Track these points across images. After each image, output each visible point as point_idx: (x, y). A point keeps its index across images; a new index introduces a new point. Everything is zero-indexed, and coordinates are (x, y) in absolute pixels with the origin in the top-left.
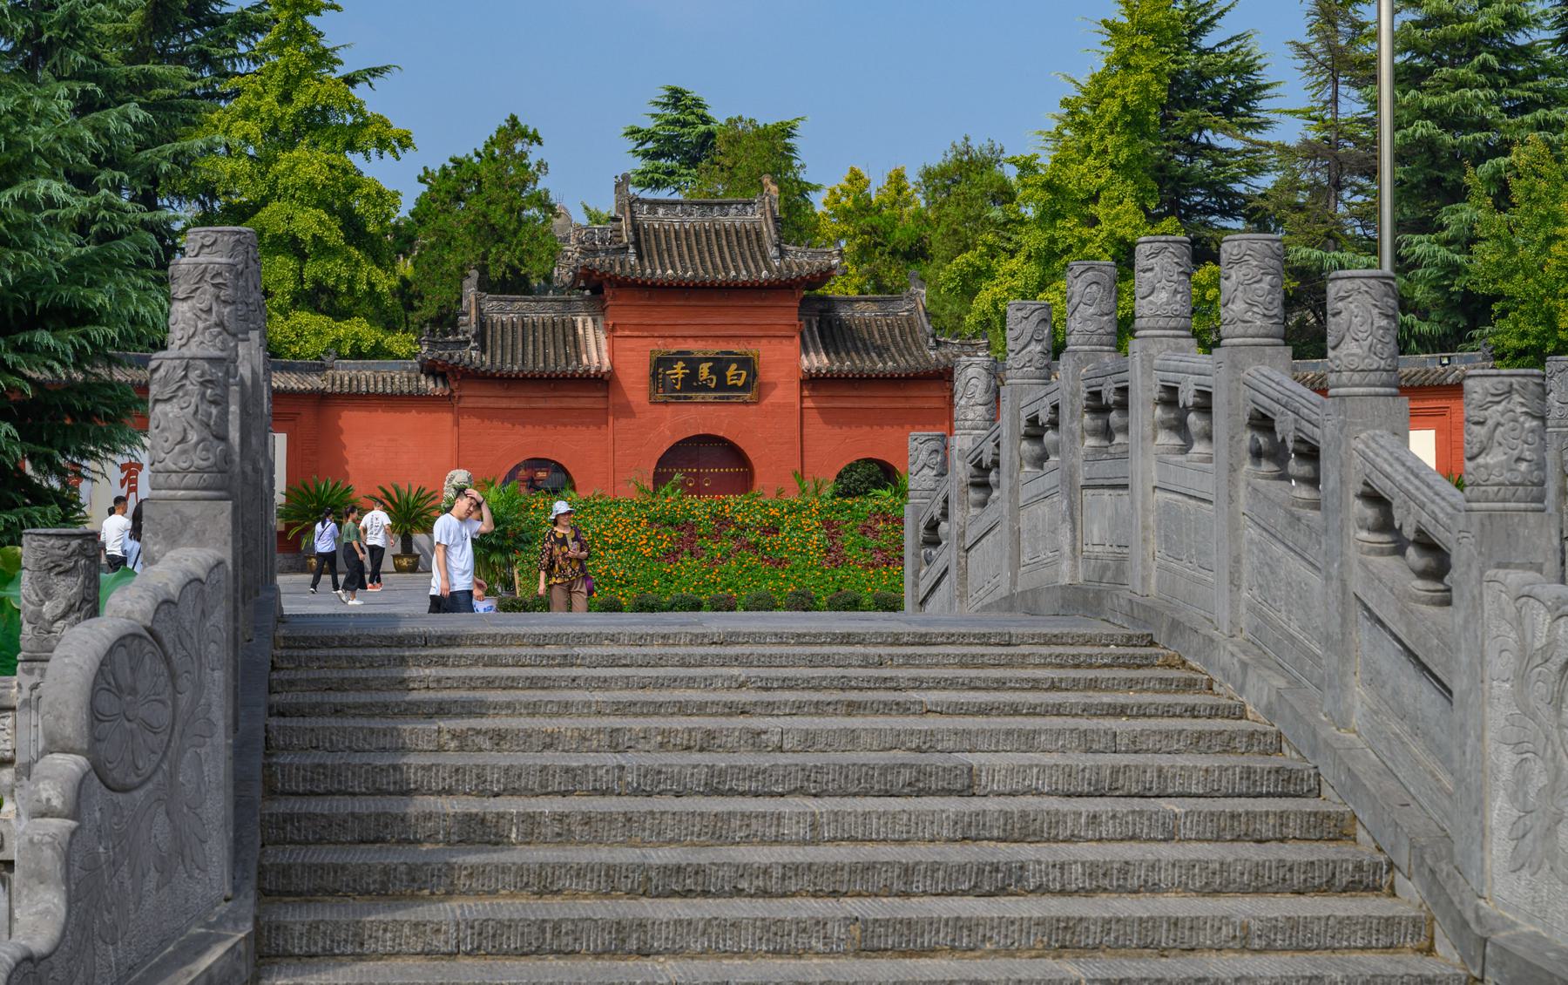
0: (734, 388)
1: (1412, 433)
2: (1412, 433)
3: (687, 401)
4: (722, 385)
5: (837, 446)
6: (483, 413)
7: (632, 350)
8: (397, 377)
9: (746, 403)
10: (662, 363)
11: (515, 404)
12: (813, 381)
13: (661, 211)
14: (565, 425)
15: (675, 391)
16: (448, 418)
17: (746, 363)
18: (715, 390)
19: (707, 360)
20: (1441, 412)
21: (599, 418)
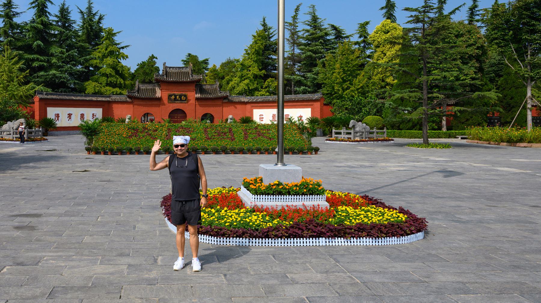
1: (254, 110)
2: (254, 110)
5: (201, 111)
8: (123, 98)
10: (170, 96)
12: (197, 99)
16: (132, 106)
17: (185, 96)
20: (312, 105)
21: (159, 106)
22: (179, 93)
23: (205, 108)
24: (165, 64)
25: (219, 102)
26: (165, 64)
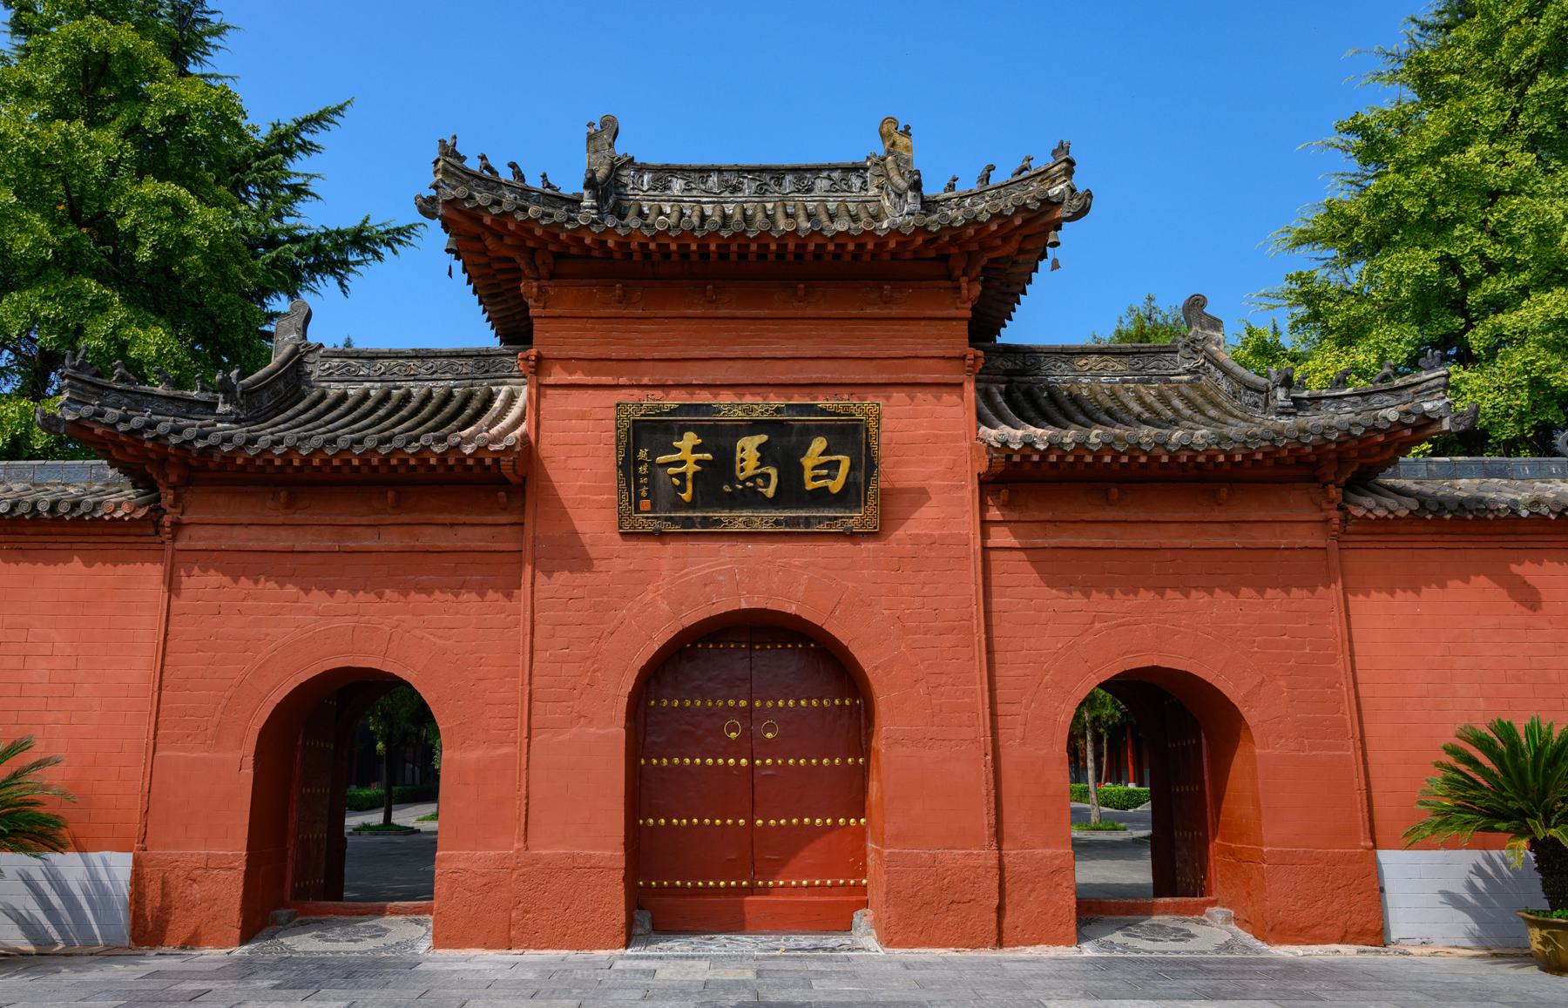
0: (821, 497)
3: (711, 532)
4: (792, 492)
6: (237, 563)
7: (582, 416)
9: (851, 536)
10: (644, 436)
11: (304, 541)
13: (677, 185)
14: (428, 591)
15: (679, 505)
16: (148, 576)
18: (774, 503)
19: (754, 427)
21: (501, 573)
22: (764, 404)
23: (1123, 604)
25: (1295, 525)
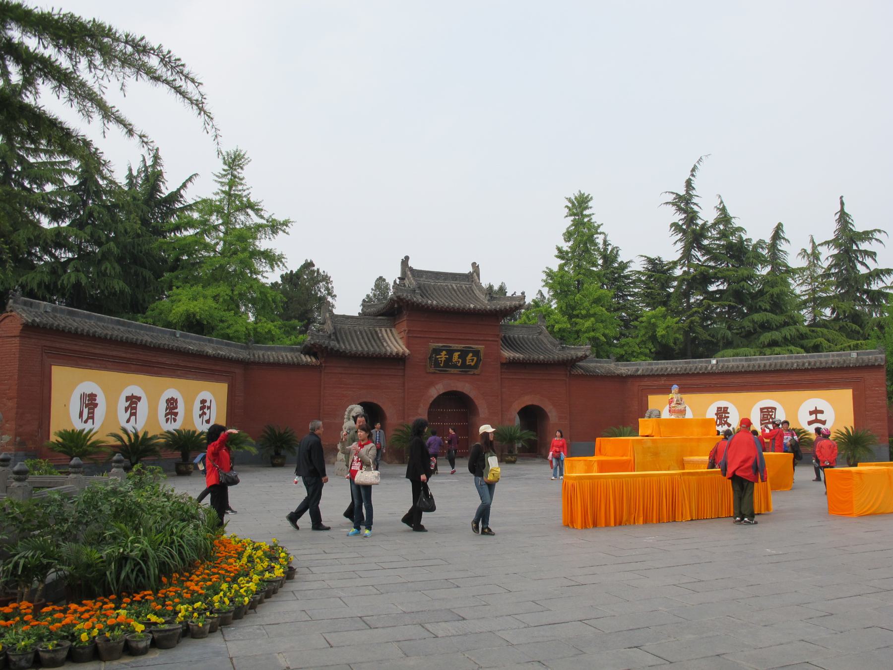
0: (470, 367)
17: (476, 353)
24: (405, 261)
26: (405, 261)
